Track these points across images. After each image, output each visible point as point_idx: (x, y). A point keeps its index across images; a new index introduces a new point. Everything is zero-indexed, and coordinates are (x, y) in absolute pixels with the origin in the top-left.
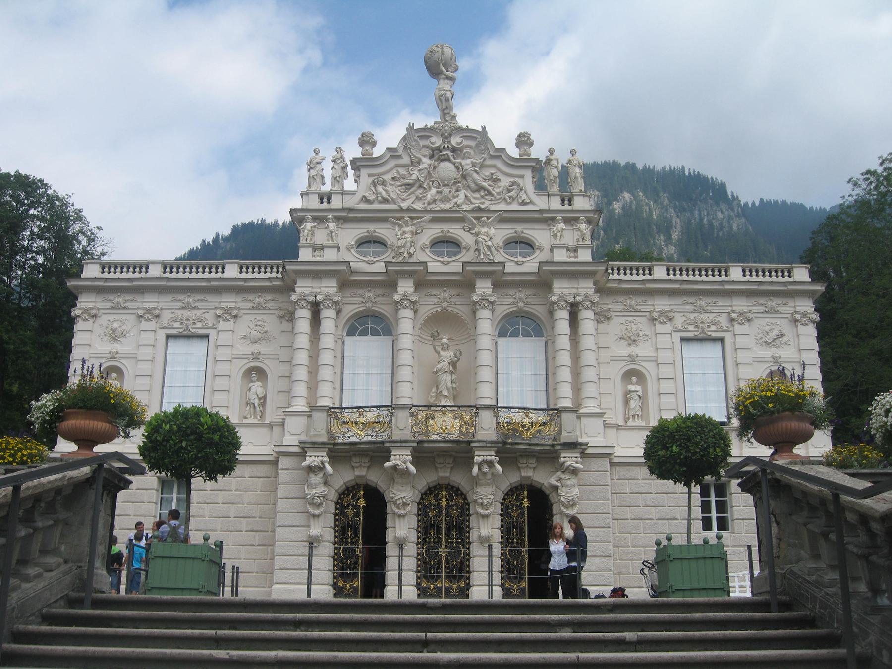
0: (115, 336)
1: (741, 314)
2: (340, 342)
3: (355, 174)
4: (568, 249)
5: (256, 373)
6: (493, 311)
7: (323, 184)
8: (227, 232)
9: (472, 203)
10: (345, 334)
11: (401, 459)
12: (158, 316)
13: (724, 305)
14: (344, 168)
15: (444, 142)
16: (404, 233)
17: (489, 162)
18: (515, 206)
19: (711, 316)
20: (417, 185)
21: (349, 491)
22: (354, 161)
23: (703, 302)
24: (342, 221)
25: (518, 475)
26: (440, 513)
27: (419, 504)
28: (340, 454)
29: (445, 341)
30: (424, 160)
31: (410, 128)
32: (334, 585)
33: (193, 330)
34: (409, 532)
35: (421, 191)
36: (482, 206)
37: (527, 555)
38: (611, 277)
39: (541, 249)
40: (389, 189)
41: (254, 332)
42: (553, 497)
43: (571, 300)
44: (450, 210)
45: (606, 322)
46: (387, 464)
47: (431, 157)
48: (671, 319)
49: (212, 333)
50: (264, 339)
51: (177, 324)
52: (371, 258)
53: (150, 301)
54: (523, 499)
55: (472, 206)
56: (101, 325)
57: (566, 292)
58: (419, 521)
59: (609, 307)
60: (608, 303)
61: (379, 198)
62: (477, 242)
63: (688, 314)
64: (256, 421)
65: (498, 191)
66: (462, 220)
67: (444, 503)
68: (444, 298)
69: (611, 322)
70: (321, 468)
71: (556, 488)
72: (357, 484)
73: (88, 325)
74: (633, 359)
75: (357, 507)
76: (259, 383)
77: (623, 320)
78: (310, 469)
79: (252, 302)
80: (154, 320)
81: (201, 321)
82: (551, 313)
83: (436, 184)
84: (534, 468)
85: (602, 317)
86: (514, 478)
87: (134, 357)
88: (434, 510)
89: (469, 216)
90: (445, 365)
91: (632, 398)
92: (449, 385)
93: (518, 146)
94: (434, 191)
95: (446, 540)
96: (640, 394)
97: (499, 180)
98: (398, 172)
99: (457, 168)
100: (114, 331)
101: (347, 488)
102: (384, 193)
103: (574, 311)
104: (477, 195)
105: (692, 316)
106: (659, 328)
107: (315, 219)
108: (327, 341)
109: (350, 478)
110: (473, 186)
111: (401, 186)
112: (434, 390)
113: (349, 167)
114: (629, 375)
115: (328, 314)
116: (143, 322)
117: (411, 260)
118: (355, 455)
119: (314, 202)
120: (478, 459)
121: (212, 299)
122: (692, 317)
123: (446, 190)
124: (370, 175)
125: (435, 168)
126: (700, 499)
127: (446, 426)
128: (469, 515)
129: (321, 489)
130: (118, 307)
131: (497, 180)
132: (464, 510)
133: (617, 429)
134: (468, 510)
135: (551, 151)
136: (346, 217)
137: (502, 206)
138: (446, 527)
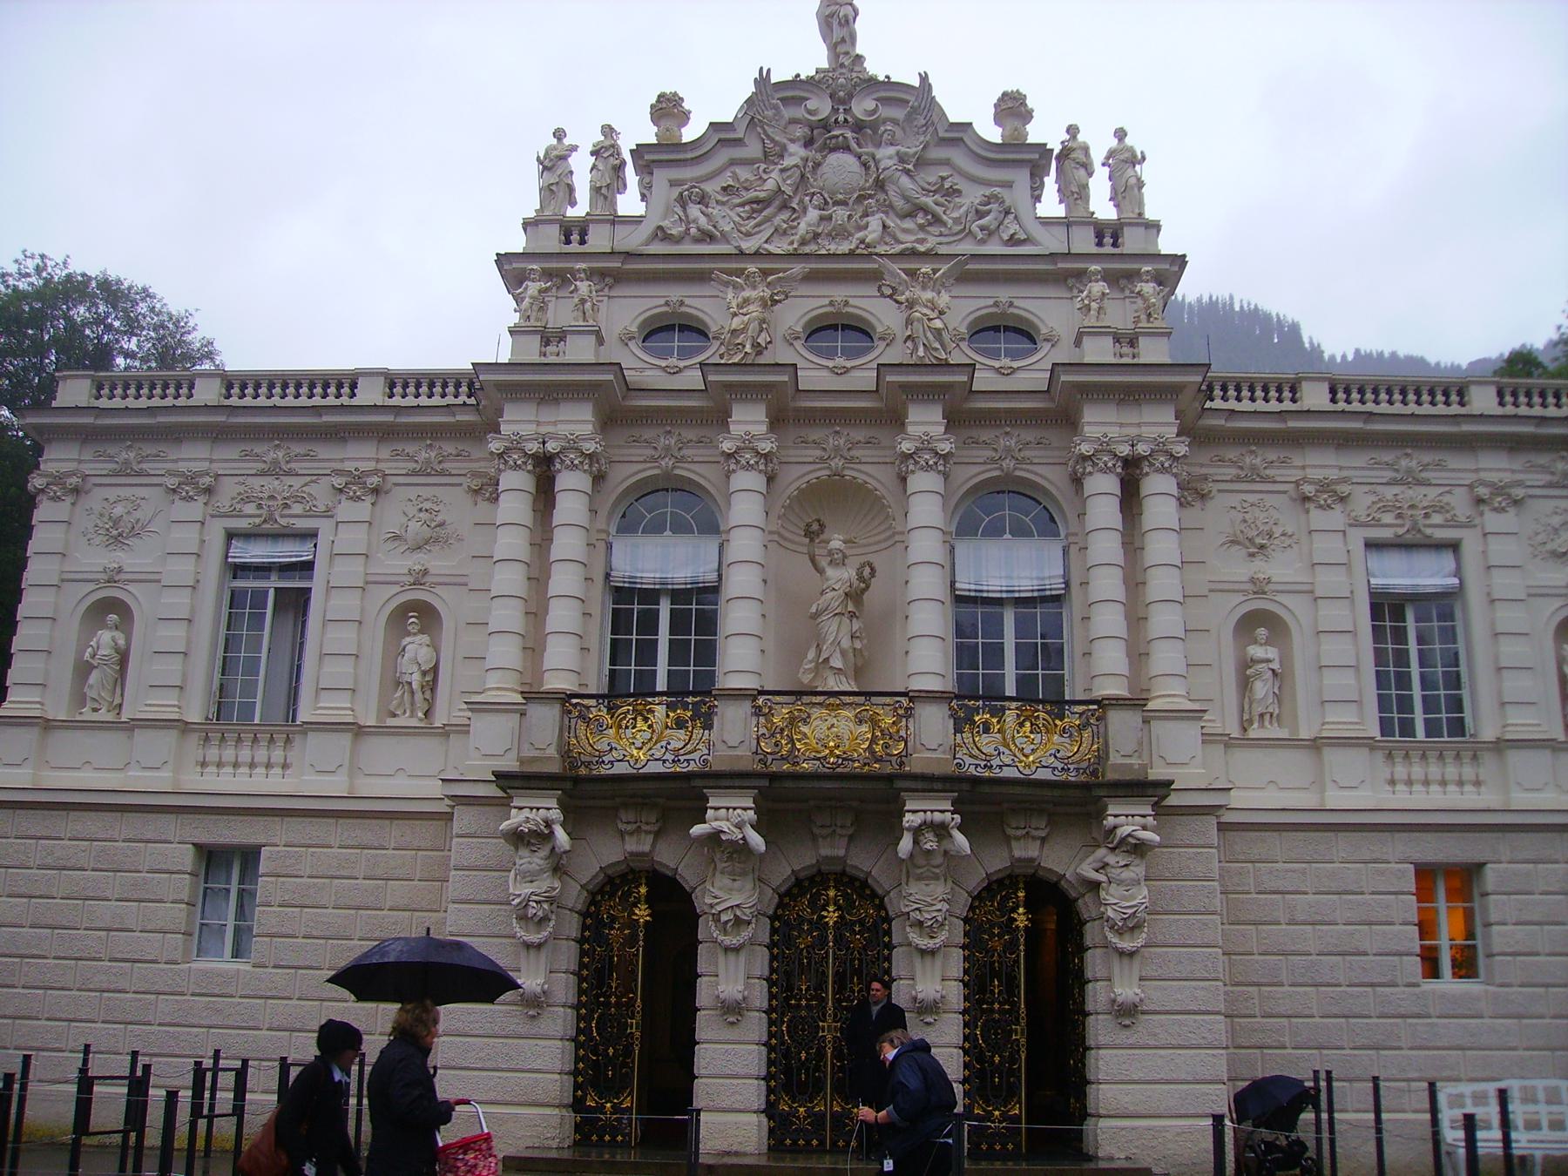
0: (119, 535)
1: (1498, 489)
2: (601, 546)
3: (641, 182)
4: (1117, 339)
5: (418, 615)
6: (946, 476)
7: (573, 203)
9: (899, 242)
10: (613, 530)
11: (730, 815)
12: (209, 491)
13: (1461, 466)
14: (619, 168)
15: (835, 110)
16: (746, 301)
17: (936, 153)
18: (994, 248)
19: (1433, 493)
20: (777, 203)
21: (613, 886)
22: (639, 151)
23: (1411, 461)
24: (609, 280)
25: (1006, 854)
26: (823, 942)
27: (773, 918)
29: (836, 544)
30: (792, 148)
31: (763, 80)
32: (577, 1105)
33: (283, 522)
34: (747, 986)
35: (785, 215)
36: (922, 248)
37: (1023, 1041)
38: (1208, 405)
39: (1052, 341)
40: (715, 211)
41: (414, 526)
42: (1086, 907)
43: (1124, 450)
44: (851, 255)
45: (1198, 504)
46: (697, 830)
47: (808, 143)
48: (1342, 499)
49: (324, 527)
50: (437, 541)
51: (250, 509)
52: (673, 361)
53: (194, 457)
54: (1014, 910)
55: (898, 248)
56: (90, 511)
57: (1113, 432)
58: (773, 958)
59: (1204, 471)
61: (693, 231)
62: (909, 322)
63: (1379, 489)
64: (414, 722)
65: (955, 215)
66: (875, 277)
67: (831, 915)
68: (837, 449)
69: (1210, 504)
71: (1095, 886)
72: (632, 870)
73: (62, 510)
74: (1259, 587)
75: (634, 924)
76: (425, 638)
77: (1234, 500)
78: (518, 838)
79: (411, 458)
80: (202, 499)
81: (300, 500)
82: (1077, 481)
83: (817, 200)
84: (1043, 840)
85: (1192, 493)
86: (996, 861)
88: (810, 932)
89: (895, 267)
90: (833, 599)
91: (1259, 675)
92: (846, 643)
93: (999, 119)
94: (813, 214)
95: (837, 1002)
96: (1275, 666)
97: (958, 192)
98: (735, 177)
99: (865, 165)
100: (116, 522)
101: (610, 880)
102: (703, 221)
104: (908, 224)
105: (1389, 492)
106: (1318, 518)
107: (548, 274)
108: (567, 543)
109: (614, 859)
110: (899, 203)
111: (742, 205)
112: (811, 655)
113: (630, 170)
114: (1249, 624)
115: (571, 484)
116: (178, 503)
117: (761, 360)
118: (625, 806)
119: (551, 240)
120: (910, 820)
121: (328, 453)
122: (1389, 497)
123: (840, 214)
124: (673, 183)
125: (817, 165)
126: (1415, 905)
127: (833, 735)
128: (890, 947)
129: (546, 884)
130: (125, 471)
131: (954, 192)
133: (1227, 746)
134: (889, 933)
135: (1072, 130)
136: (620, 271)
137: (967, 247)
138: (836, 974)
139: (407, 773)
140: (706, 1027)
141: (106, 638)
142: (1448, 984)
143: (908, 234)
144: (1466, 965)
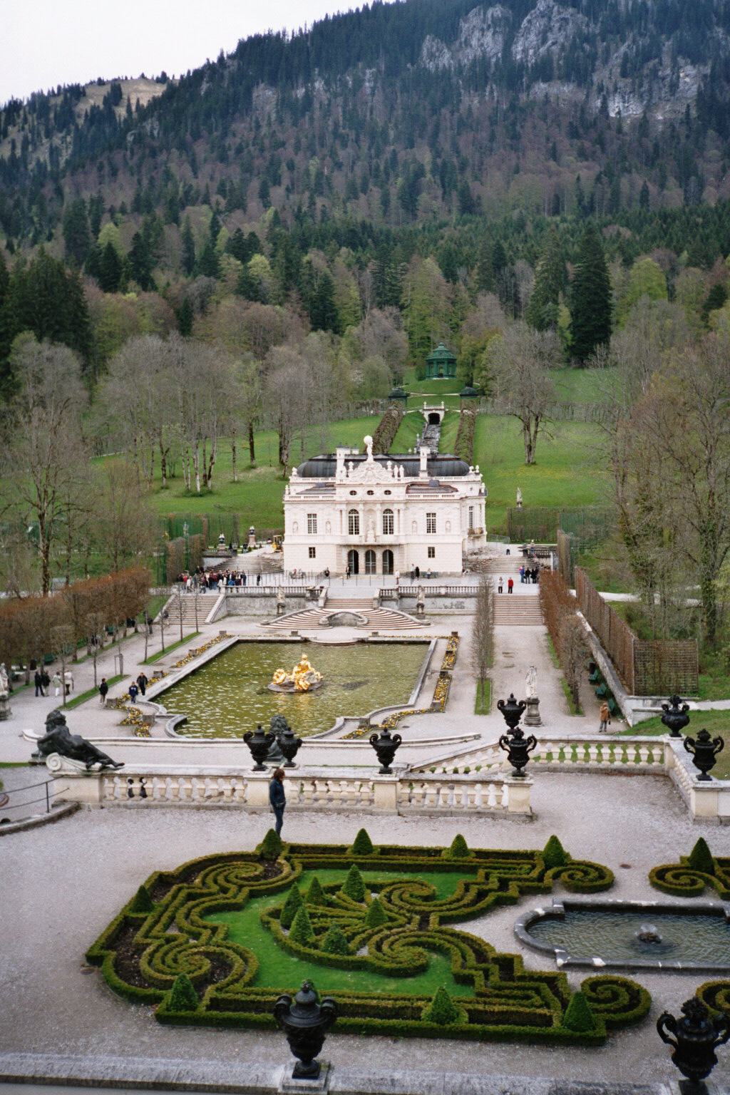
0: (295, 514)
8: (231, 48)
53: (302, 506)
60: (409, 505)
127: (371, 541)
139: (329, 540)
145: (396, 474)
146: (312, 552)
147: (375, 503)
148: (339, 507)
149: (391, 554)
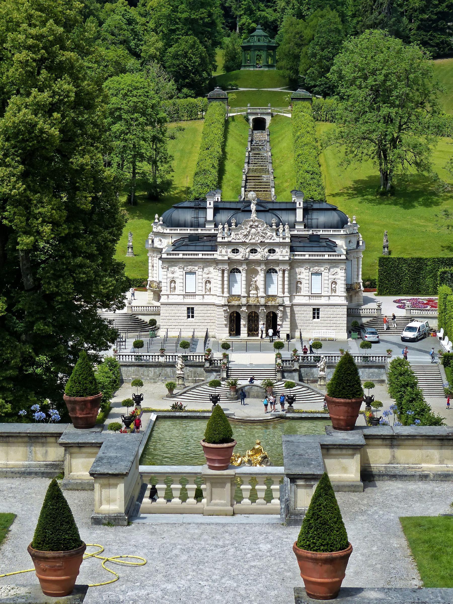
11: (244, 309)
28: (230, 306)
49: (197, 272)
70: (227, 310)
87: (178, 278)
103: (284, 271)
108: (226, 279)
123: (254, 236)
132: (258, 316)
140: (242, 326)
141: (173, 285)
142: (316, 320)
143: (262, 239)
144: (318, 318)
145: (281, 230)
146: (191, 312)
147: (258, 263)
148: (220, 266)
149: (275, 316)
